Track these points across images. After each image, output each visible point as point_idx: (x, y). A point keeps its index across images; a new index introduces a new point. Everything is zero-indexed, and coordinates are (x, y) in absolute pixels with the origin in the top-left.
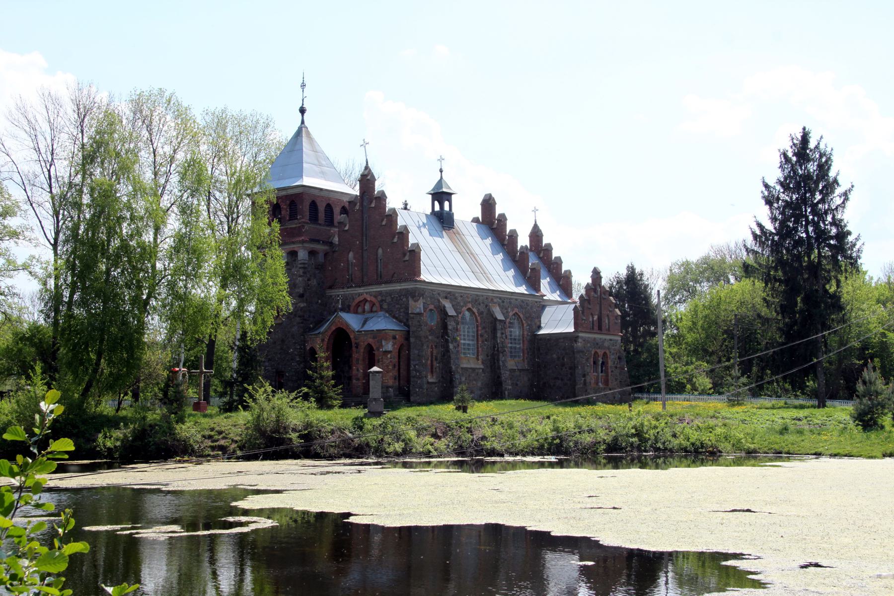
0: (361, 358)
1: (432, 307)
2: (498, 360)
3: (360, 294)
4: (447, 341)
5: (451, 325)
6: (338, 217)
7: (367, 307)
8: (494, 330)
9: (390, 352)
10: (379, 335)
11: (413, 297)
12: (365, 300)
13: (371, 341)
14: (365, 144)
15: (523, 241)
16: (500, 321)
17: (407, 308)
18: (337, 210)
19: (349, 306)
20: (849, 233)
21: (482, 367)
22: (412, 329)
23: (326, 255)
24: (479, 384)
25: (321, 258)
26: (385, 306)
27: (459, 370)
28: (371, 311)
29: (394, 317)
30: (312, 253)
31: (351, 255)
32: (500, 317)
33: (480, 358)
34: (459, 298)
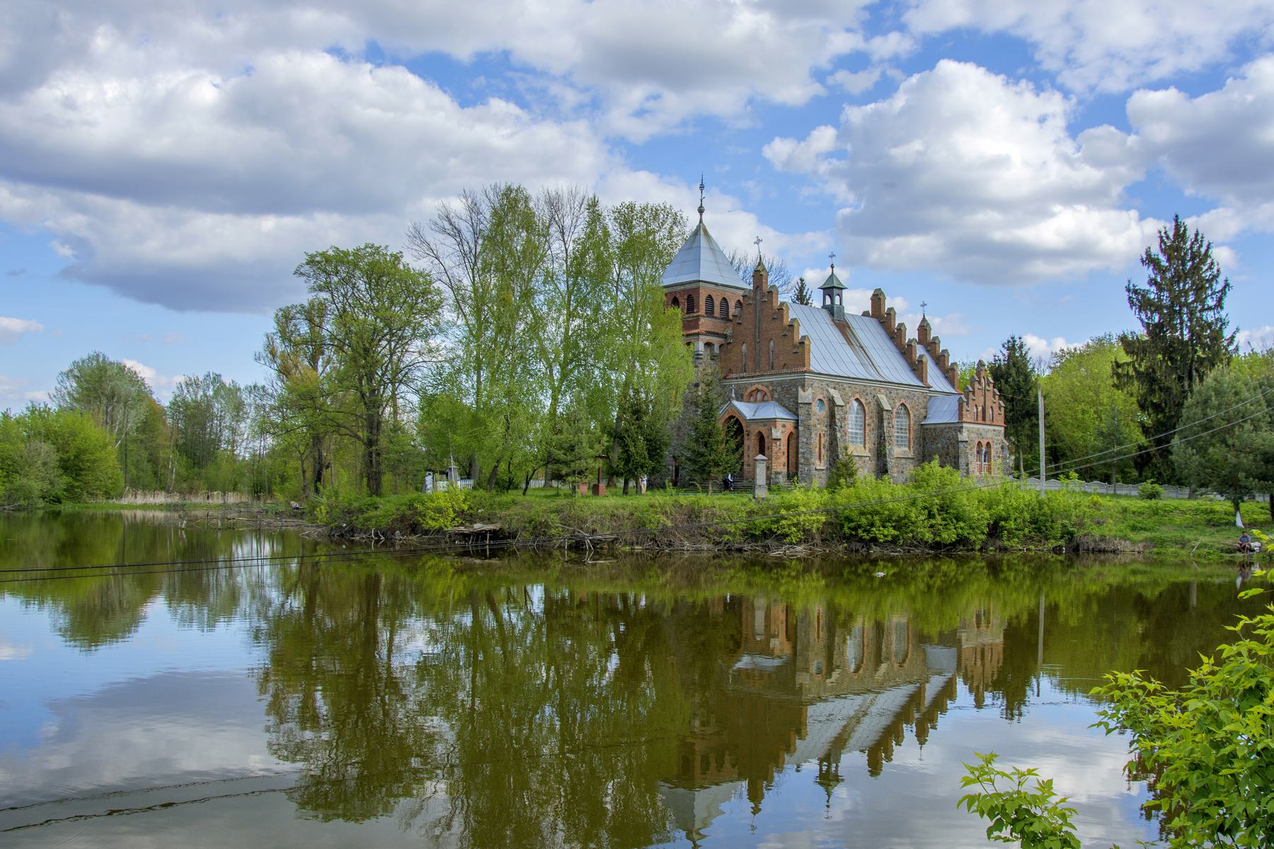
1: (821, 397)
3: (752, 384)
6: (732, 310)
7: (759, 396)
8: (881, 420)
10: (771, 422)
12: (758, 390)
15: (911, 334)
17: (797, 398)
18: (732, 304)
19: (742, 396)
22: (801, 418)
25: (716, 350)
28: (763, 400)
30: (708, 345)
31: (744, 347)
32: (887, 406)
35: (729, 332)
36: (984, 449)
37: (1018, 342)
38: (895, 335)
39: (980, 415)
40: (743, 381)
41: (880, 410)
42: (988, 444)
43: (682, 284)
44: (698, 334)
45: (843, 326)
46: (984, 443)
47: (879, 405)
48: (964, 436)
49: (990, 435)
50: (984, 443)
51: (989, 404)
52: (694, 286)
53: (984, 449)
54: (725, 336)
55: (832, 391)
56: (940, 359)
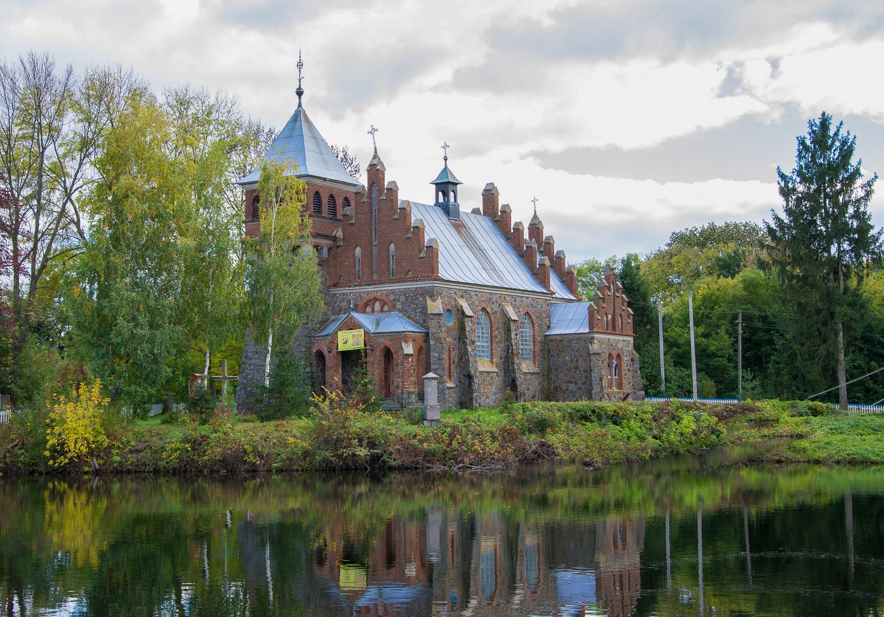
0: (377, 361)
2: (513, 363)
4: (465, 344)
5: (468, 325)
7: (377, 306)
8: (508, 331)
9: (411, 355)
10: (400, 337)
11: (432, 296)
13: (388, 343)
14: (373, 131)
16: (515, 321)
18: (339, 201)
20: (872, 227)
21: (496, 370)
22: (432, 330)
24: (494, 389)
26: (399, 305)
27: (478, 374)
28: (382, 311)
29: (409, 317)
31: (358, 251)
32: (514, 317)
33: (495, 360)
34: (474, 297)
38: (511, 236)
39: (610, 323)
41: (508, 321)
42: (619, 356)
45: (459, 227)
47: (504, 314)
48: (595, 347)
51: (618, 311)
53: (615, 362)
56: (557, 262)
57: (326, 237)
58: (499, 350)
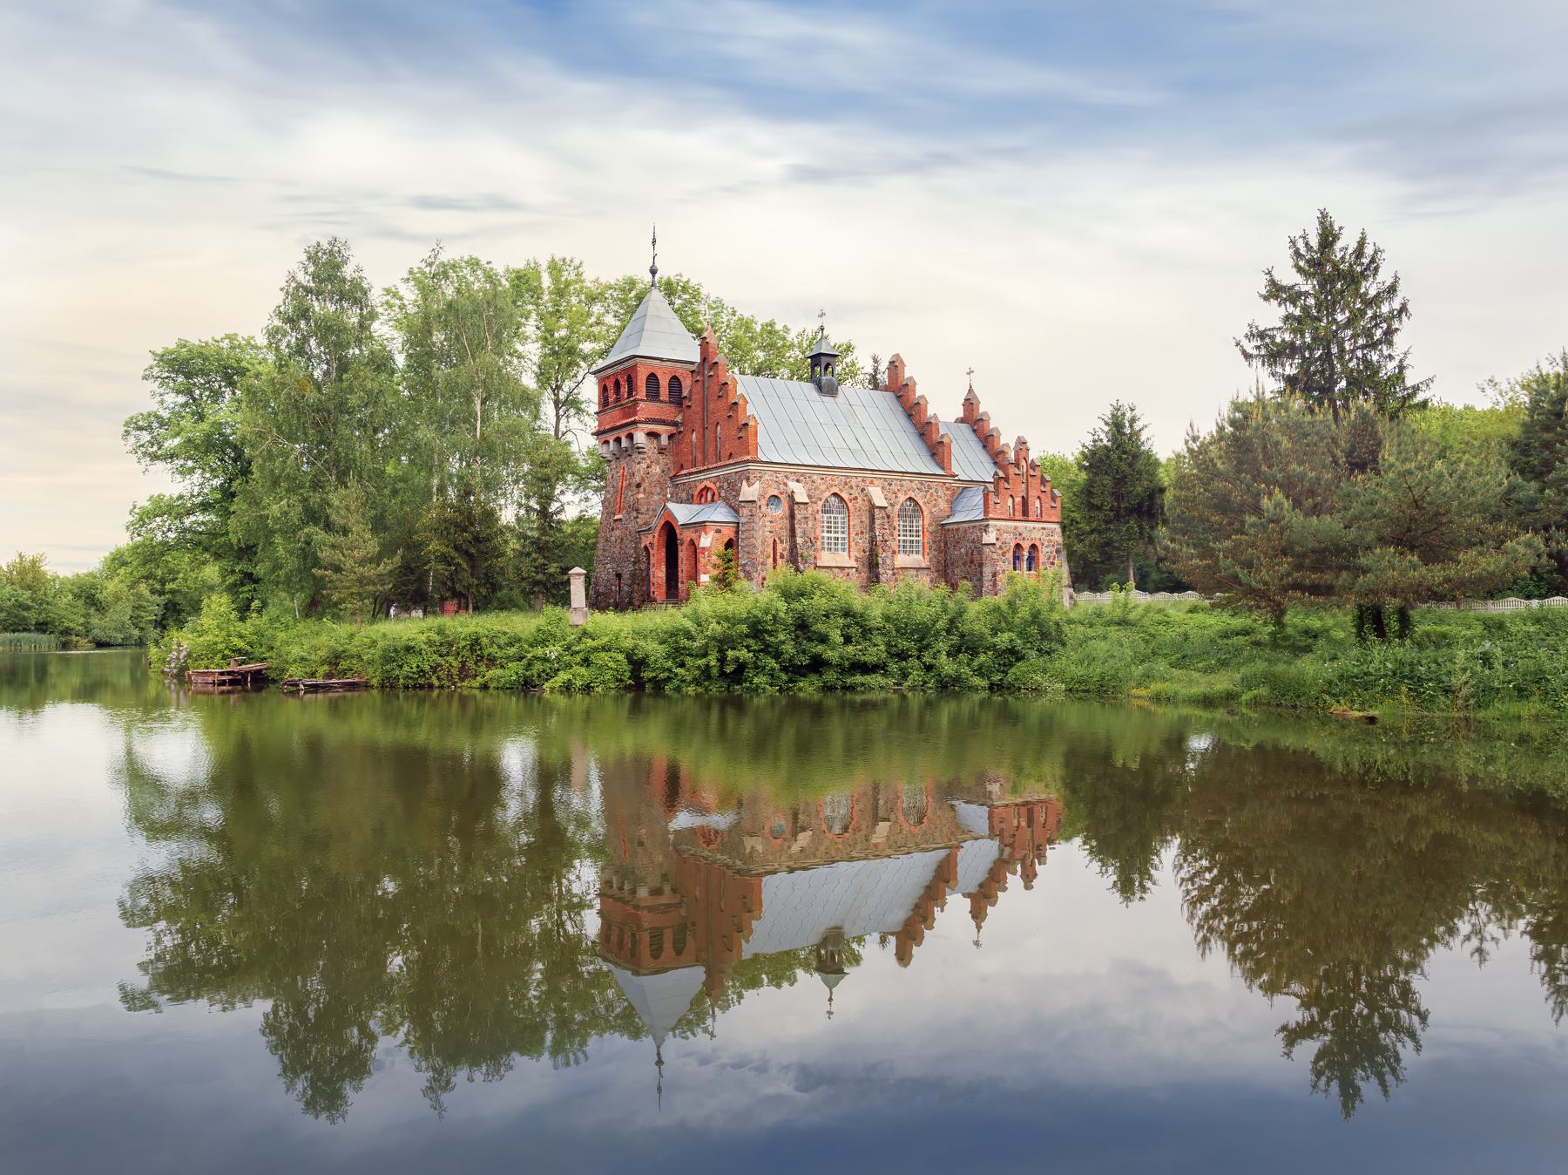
1: (776, 493)
10: (702, 526)
12: (707, 489)
23: (671, 437)
25: (664, 440)
30: (652, 435)
35: (679, 419)
36: (1026, 554)
37: (1129, 415)
39: (1019, 508)
40: (693, 478)
42: (1034, 546)
43: (620, 362)
44: (635, 423)
46: (1026, 545)
48: (989, 538)
49: (1037, 535)
50: (1026, 545)
51: (1033, 493)
52: (626, 365)
54: (675, 424)
55: (793, 485)
57: (663, 422)
58: (863, 541)
